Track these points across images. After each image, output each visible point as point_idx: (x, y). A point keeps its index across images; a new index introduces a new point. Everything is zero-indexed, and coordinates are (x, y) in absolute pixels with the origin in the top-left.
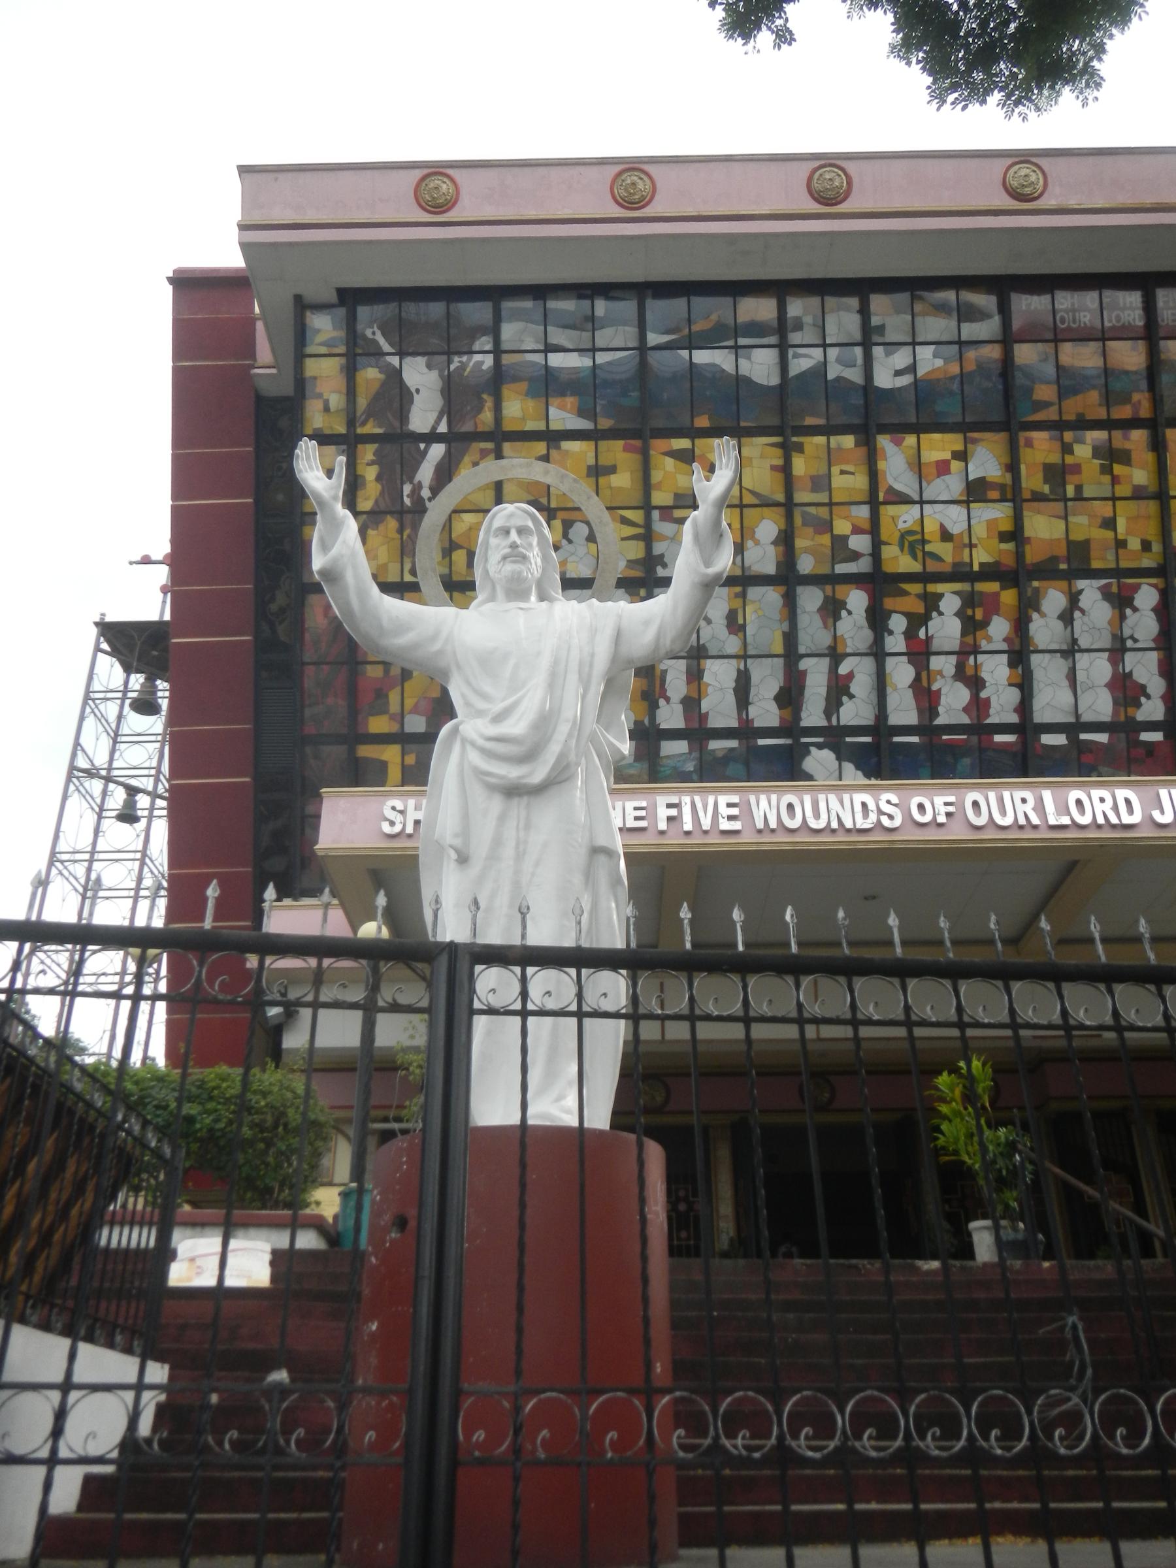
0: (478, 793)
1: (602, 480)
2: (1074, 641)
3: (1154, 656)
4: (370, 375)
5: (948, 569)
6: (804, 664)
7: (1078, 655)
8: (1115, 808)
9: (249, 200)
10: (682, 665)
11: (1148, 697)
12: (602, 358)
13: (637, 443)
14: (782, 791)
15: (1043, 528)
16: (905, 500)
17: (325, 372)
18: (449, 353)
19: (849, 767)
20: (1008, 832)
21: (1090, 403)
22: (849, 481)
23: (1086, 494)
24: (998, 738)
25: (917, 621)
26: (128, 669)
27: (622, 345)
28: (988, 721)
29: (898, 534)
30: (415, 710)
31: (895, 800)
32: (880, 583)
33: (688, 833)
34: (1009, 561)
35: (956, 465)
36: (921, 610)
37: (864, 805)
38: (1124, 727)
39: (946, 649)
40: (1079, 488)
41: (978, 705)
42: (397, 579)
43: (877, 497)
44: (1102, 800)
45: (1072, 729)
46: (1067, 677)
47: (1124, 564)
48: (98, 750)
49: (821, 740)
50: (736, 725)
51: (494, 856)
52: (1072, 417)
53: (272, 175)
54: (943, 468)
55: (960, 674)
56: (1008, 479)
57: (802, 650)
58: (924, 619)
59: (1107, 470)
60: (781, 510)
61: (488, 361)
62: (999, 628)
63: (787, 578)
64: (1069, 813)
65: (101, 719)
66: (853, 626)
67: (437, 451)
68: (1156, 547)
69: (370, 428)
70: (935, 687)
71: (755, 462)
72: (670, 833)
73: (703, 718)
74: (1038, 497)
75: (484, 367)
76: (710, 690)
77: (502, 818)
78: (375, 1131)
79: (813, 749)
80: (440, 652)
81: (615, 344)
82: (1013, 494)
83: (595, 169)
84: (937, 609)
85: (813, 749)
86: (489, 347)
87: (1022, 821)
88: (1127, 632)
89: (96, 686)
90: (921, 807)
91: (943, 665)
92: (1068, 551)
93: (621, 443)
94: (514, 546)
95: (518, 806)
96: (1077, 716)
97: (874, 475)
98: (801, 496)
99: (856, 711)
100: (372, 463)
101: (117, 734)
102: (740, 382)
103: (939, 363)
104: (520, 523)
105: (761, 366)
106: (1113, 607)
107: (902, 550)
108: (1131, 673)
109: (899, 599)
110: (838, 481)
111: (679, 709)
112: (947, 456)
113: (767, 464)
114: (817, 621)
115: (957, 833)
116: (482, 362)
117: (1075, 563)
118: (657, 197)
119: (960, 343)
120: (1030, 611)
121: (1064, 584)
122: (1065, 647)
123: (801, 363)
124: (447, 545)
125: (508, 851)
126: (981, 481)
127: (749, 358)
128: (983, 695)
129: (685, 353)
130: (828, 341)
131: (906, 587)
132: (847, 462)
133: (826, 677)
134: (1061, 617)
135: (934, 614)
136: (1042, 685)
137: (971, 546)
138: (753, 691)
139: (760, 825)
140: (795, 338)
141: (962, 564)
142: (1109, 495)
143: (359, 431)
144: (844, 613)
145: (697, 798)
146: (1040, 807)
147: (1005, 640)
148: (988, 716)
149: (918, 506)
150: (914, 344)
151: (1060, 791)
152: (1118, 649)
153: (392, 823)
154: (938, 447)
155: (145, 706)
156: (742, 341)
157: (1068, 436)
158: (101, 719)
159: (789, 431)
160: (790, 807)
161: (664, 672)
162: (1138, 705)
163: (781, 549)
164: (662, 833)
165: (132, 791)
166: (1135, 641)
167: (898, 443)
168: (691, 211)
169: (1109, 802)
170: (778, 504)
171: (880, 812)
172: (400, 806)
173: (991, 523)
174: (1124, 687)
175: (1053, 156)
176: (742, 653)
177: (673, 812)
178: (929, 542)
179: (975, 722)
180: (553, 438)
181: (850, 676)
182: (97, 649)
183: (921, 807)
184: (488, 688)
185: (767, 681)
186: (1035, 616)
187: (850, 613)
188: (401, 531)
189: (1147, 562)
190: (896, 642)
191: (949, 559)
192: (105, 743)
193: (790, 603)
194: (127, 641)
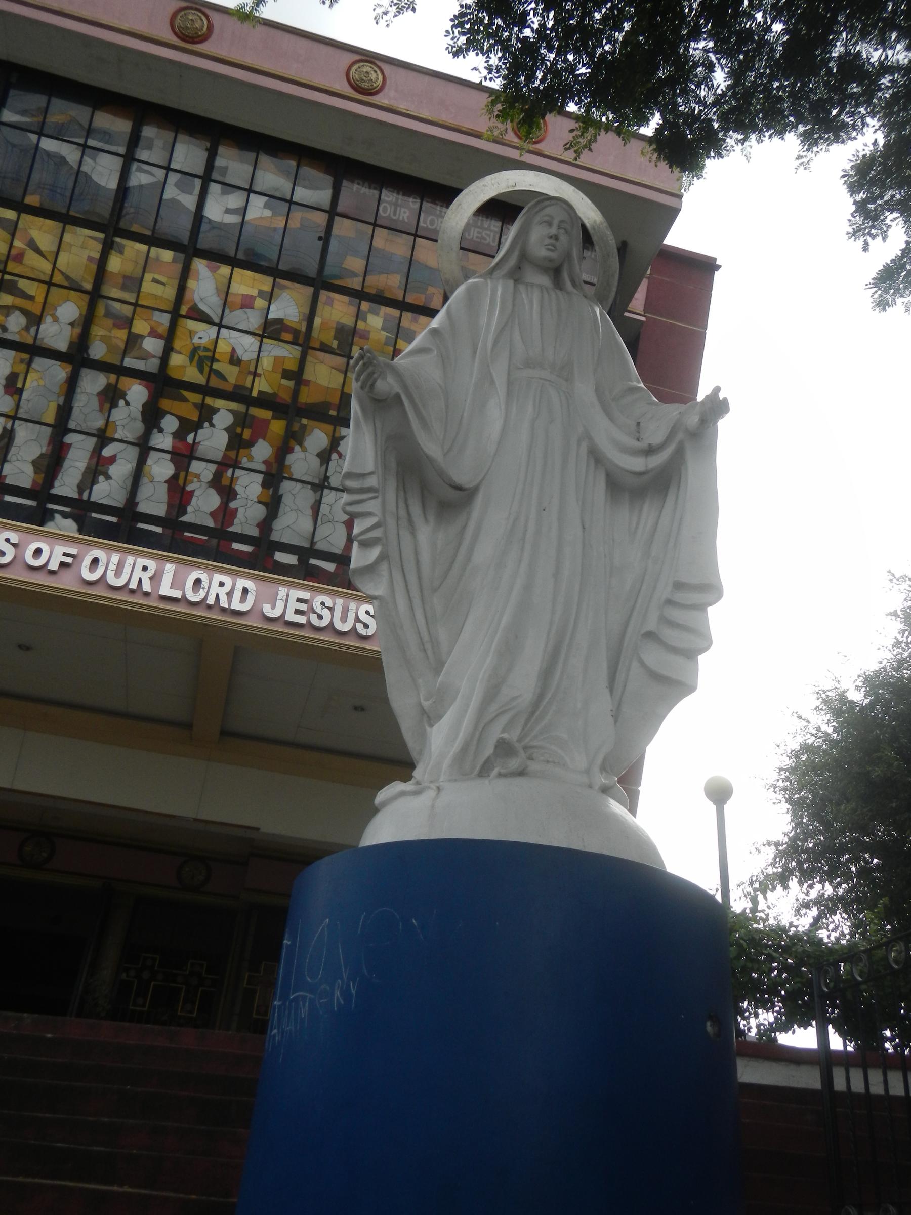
2: (326, 478)
5: (229, 388)
6: (70, 438)
7: (326, 491)
8: (230, 594)
15: (323, 374)
16: (204, 318)
20: (117, 592)
22: (158, 289)
24: (236, 546)
25: (187, 427)
28: (231, 529)
32: (162, 384)
34: (286, 397)
35: (260, 303)
36: (196, 419)
41: (225, 514)
45: (305, 553)
46: (312, 508)
55: (216, 483)
57: (72, 425)
58: (198, 426)
62: (262, 451)
64: (183, 589)
66: (127, 417)
79: (58, 517)
82: (303, 339)
84: (210, 421)
85: (58, 517)
90: (38, 552)
91: (202, 470)
92: (340, 400)
96: (313, 543)
97: (182, 289)
99: (109, 491)
103: (268, 213)
105: (104, 172)
107: (191, 359)
110: (148, 286)
112: (254, 292)
113: (85, 254)
115: (66, 582)
119: (291, 202)
120: (292, 443)
121: (330, 428)
122: (316, 481)
126: (279, 321)
128: (232, 505)
129: (34, 137)
130: (172, 166)
131: (186, 394)
133: (88, 455)
134: (318, 455)
135: (206, 424)
136: (287, 509)
137: (255, 374)
138: (13, 450)
140: (143, 154)
146: (156, 579)
148: (232, 524)
149: (216, 328)
150: (250, 191)
151: (183, 568)
154: (246, 283)
156: (91, 142)
157: (365, 306)
167: (214, 270)
169: (227, 588)
170: (85, 292)
175: (394, 65)
176: (12, 414)
178: (218, 361)
179: (219, 527)
183: (38, 552)
186: (297, 448)
187: (127, 403)
190: (163, 440)
191: (232, 380)
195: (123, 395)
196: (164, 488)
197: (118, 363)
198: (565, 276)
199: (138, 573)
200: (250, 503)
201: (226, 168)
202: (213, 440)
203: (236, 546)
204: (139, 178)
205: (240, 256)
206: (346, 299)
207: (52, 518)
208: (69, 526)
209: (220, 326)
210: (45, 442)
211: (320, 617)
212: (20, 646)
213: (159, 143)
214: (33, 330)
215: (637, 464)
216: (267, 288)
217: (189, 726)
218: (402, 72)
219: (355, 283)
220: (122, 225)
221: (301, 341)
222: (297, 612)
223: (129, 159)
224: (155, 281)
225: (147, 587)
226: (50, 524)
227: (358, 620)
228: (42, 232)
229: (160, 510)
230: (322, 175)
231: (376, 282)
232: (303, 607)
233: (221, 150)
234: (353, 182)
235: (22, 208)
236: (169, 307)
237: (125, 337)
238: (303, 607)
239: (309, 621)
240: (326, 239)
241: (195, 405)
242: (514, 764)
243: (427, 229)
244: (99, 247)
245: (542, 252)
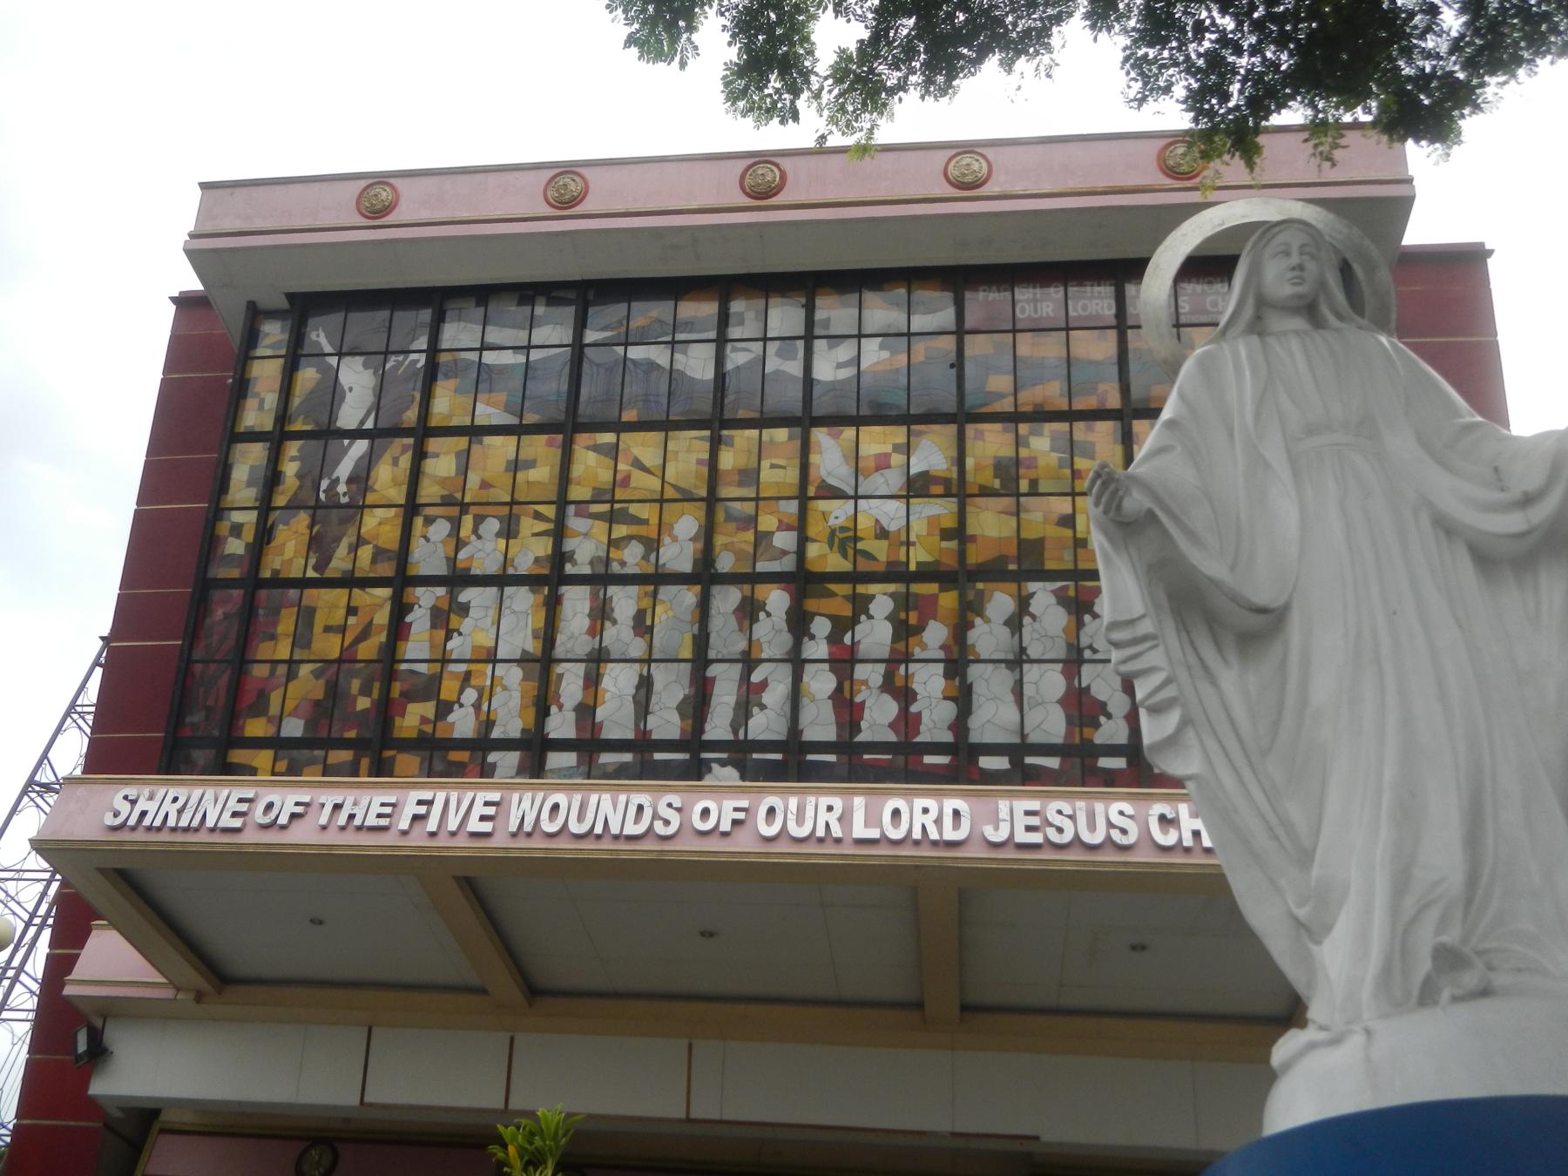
2: (1023, 650)
4: (308, 376)
5: (882, 568)
6: (713, 671)
7: (1026, 667)
8: (938, 822)
9: (204, 212)
10: (580, 668)
11: (1109, 716)
16: (837, 494)
17: (266, 373)
22: (778, 474)
23: (1041, 490)
24: (929, 759)
25: (842, 626)
28: (918, 739)
30: (295, 713)
31: (677, 803)
33: (433, 834)
34: (951, 562)
35: (897, 459)
36: (850, 614)
37: (640, 808)
39: (874, 656)
40: (1034, 483)
41: (907, 721)
43: (807, 491)
45: (1018, 750)
46: (1013, 691)
50: (630, 735)
52: (1029, 408)
55: (888, 685)
57: (712, 654)
58: (854, 622)
61: (422, 359)
62: (936, 634)
66: (771, 632)
69: (298, 426)
70: (858, 699)
71: (681, 456)
73: (596, 727)
75: (419, 365)
76: (608, 696)
79: (715, 766)
82: (958, 489)
83: (531, 175)
85: (715, 766)
88: (1084, 641)
90: (706, 813)
93: (545, 437)
96: (1023, 736)
97: (805, 467)
98: (725, 491)
99: (766, 724)
100: (293, 459)
103: (885, 354)
105: (698, 364)
106: (1069, 613)
107: (831, 546)
108: (1088, 687)
109: (823, 601)
110: (766, 475)
111: (571, 716)
112: (889, 449)
113: (693, 458)
114: (733, 623)
115: (743, 844)
117: (1024, 564)
119: (909, 335)
120: (970, 615)
121: (1013, 587)
122: (1011, 657)
124: (354, 539)
126: (925, 476)
127: (685, 353)
128: (914, 709)
129: (620, 350)
131: (833, 587)
134: (1007, 623)
135: (863, 617)
136: (982, 699)
137: (908, 544)
138: (654, 699)
139: (513, 827)
140: (734, 332)
141: (897, 563)
142: (1068, 490)
144: (762, 615)
145: (454, 796)
148: (918, 733)
150: (860, 336)
153: (116, 815)
154: (877, 441)
156: (680, 337)
157: (1023, 428)
161: (561, 676)
162: (1097, 725)
164: (405, 833)
166: (1095, 651)
167: (836, 437)
168: (620, 208)
169: (933, 814)
173: (932, 521)
177: (422, 810)
180: (475, 432)
182: (96, 663)
183: (706, 813)
185: (671, 687)
186: (978, 621)
187: (769, 615)
188: (311, 527)
190: (817, 648)
191: (882, 557)
195: (762, 606)
197: (749, 570)
198: (1325, 310)
199: (823, 817)
200: (934, 702)
201: (828, 320)
202: (875, 634)
203: (929, 759)
204: (737, 358)
205: (865, 411)
206: (998, 426)
207: (710, 770)
208: (729, 775)
210: (686, 681)
211: (1060, 830)
212: (702, 934)
213: (750, 316)
214: (653, 557)
215: (1514, 522)
216: (902, 439)
217: (919, 1006)
219: (1006, 405)
220: (727, 415)
221: (954, 490)
222: (1029, 829)
223: (721, 341)
224: (773, 466)
225: (837, 831)
226: (708, 777)
228: (643, 446)
229: (828, 733)
230: (937, 294)
231: (1030, 397)
232: (1035, 821)
233: (819, 302)
234: (976, 290)
235: (619, 427)
236: (795, 491)
237: (752, 539)
238: (1035, 821)
239: (1047, 839)
240: (959, 364)
242: (1470, 979)
243: (1079, 318)
244: (707, 445)
245: (1288, 290)
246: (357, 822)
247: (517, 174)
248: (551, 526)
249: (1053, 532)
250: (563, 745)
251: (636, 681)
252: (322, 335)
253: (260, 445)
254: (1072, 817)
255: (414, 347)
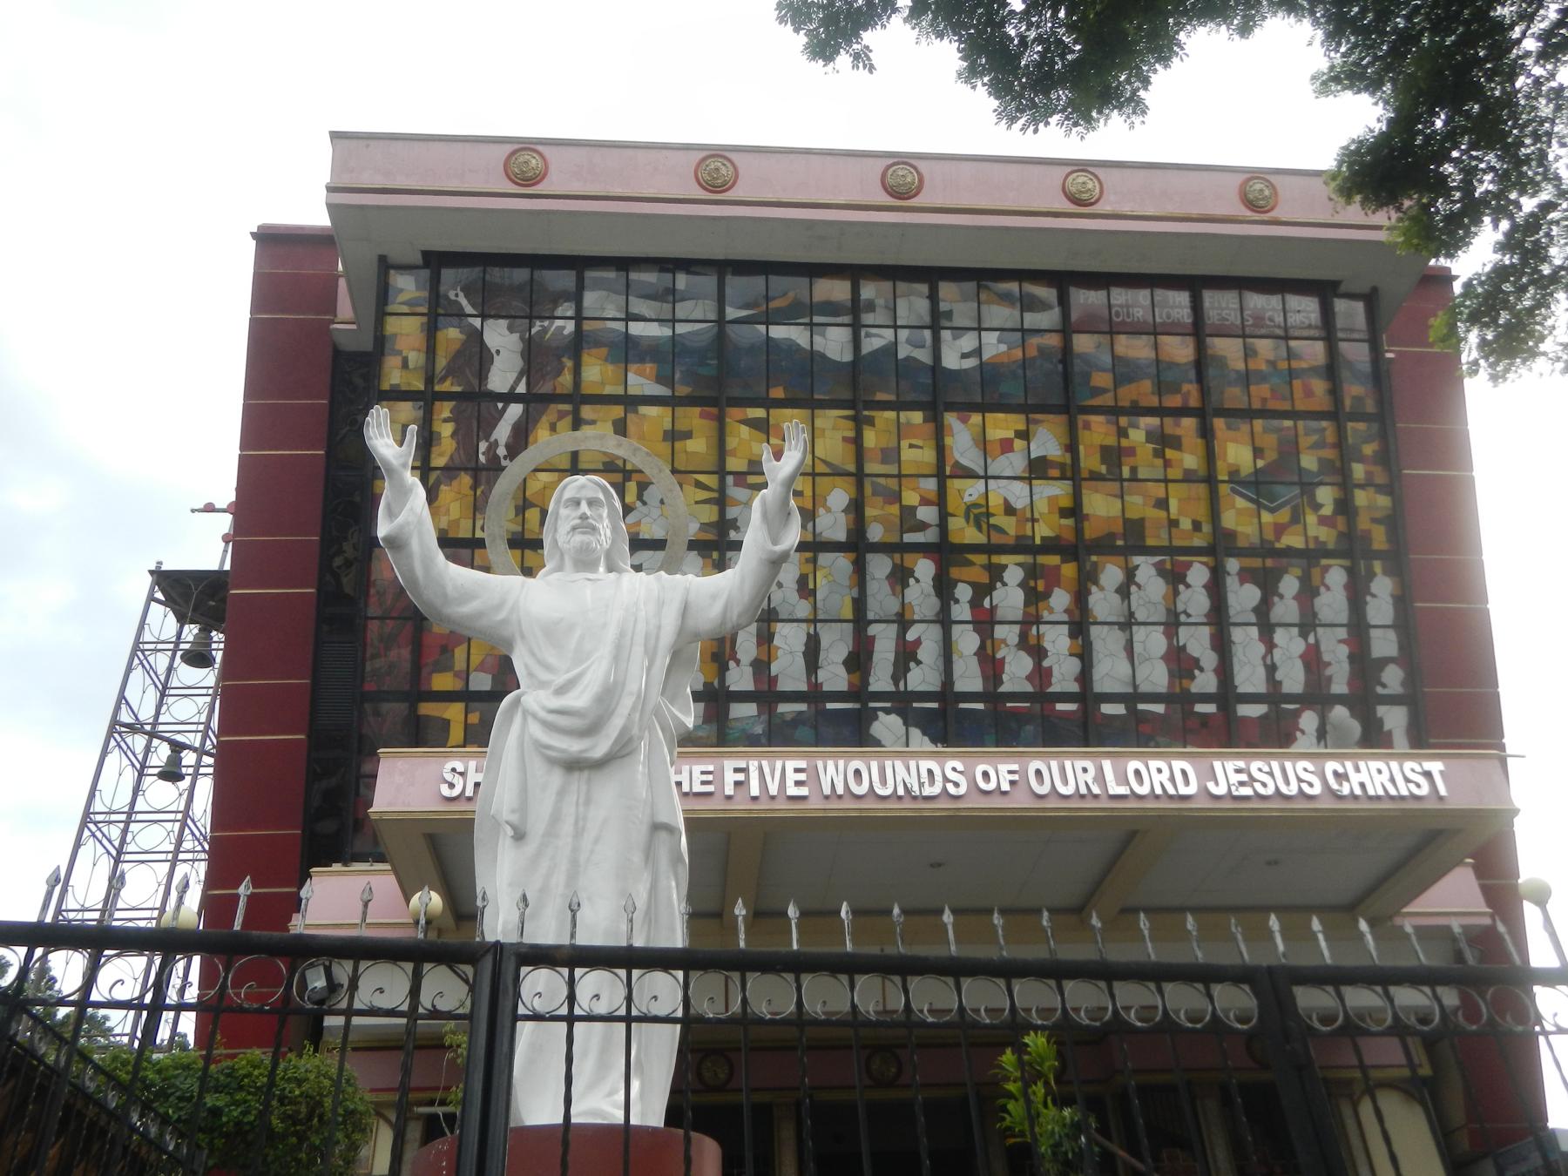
0: (537, 766)
1: (678, 445)
2: (1131, 614)
3: (1206, 631)
4: (451, 335)
5: (1011, 542)
6: (873, 630)
7: (1135, 628)
8: (1172, 779)
9: (338, 165)
11: (1202, 670)
12: (681, 329)
13: (714, 410)
14: (849, 757)
15: (1101, 506)
16: (969, 474)
17: (406, 331)
18: (531, 318)
19: (915, 733)
21: (1143, 391)
22: (918, 455)
23: (1140, 476)
24: (1060, 707)
25: (981, 591)
26: (182, 619)
27: (701, 317)
28: (1050, 690)
29: (963, 508)
30: (481, 668)
31: (960, 767)
32: (946, 553)
33: (755, 799)
34: (1069, 536)
35: (1019, 444)
37: (930, 772)
38: (1180, 698)
40: (1134, 470)
41: (1041, 674)
42: (469, 535)
43: (943, 471)
44: (1159, 771)
45: (1132, 698)
47: (1177, 543)
48: (143, 703)
49: (888, 705)
50: (804, 687)
51: (551, 833)
52: (1127, 404)
53: (362, 143)
54: (1006, 446)
56: (1068, 459)
57: (871, 616)
59: (1159, 454)
60: (852, 480)
61: (570, 327)
62: (1060, 600)
63: (857, 545)
65: (150, 670)
66: (921, 594)
67: (515, 411)
68: (1206, 528)
69: (447, 386)
70: (999, 655)
71: (827, 433)
72: (738, 798)
73: (773, 681)
74: (1095, 477)
75: (566, 332)
76: (780, 653)
77: (562, 793)
78: (420, 1116)
79: (880, 714)
80: (505, 622)
81: (694, 316)
82: (1072, 473)
83: (680, 153)
85: (880, 714)
86: (570, 313)
87: (1083, 790)
88: (1180, 608)
89: (147, 637)
90: (986, 775)
91: (1007, 634)
93: (697, 410)
94: (584, 517)
95: (578, 781)
96: (1135, 686)
97: (941, 450)
98: (872, 467)
99: (922, 678)
100: (446, 420)
101: (165, 687)
102: (814, 356)
103: (1003, 348)
104: (590, 494)
105: (834, 343)
107: (968, 521)
110: (907, 454)
111: (748, 671)
112: (1011, 434)
113: (839, 435)
114: (886, 588)
115: (1020, 801)
116: (564, 328)
117: (1130, 540)
118: (739, 182)
119: (1022, 330)
121: (1122, 559)
122: (1122, 620)
123: (874, 342)
124: (520, 503)
125: (567, 827)
126: (1043, 459)
127: (823, 335)
128: (1046, 663)
129: (762, 328)
131: (970, 557)
132: (915, 437)
133: (893, 644)
134: (1117, 591)
135: (999, 585)
137: (1033, 520)
139: (827, 791)
140: (868, 318)
141: (1024, 537)
143: (437, 388)
144: (912, 581)
145: (765, 763)
146: (1100, 777)
147: (1066, 611)
148: (1050, 684)
150: (980, 329)
152: (1172, 623)
153: (452, 786)
154: (1002, 426)
155: (198, 658)
156: (817, 319)
157: (1123, 421)
158: (150, 670)
159: (860, 406)
160: (857, 773)
162: (1193, 678)
163: (852, 516)
164: (729, 798)
165: (177, 748)
166: (1189, 616)
167: (964, 421)
170: (849, 474)
171: (946, 779)
172: (460, 768)
174: (1179, 660)
177: (741, 777)
180: (632, 402)
181: (918, 642)
182: (151, 598)
183: (986, 775)
184: (552, 659)
186: (1094, 589)
187: (917, 581)
188: (474, 488)
189: (1198, 541)
190: (961, 611)
191: (1012, 532)
192: (152, 696)
193: (860, 569)
194: (178, 589)
196: (974, 662)
199: (1082, 777)
202: (1009, 598)
207: (876, 718)
209: (986, 478)
211: (1264, 785)
218: (1116, 172)
227: (1300, 780)
232: (1244, 777)
236: (933, 471)
238: (1244, 777)
241: (983, 567)
246: (686, 788)
247: (665, 152)
248: (715, 495)
249: (1153, 514)
250: (743, 697)
251: (804, 639)
252: (461, 294)
253: (409, 404)
254: (1271, 774)
255: (559, 312)
